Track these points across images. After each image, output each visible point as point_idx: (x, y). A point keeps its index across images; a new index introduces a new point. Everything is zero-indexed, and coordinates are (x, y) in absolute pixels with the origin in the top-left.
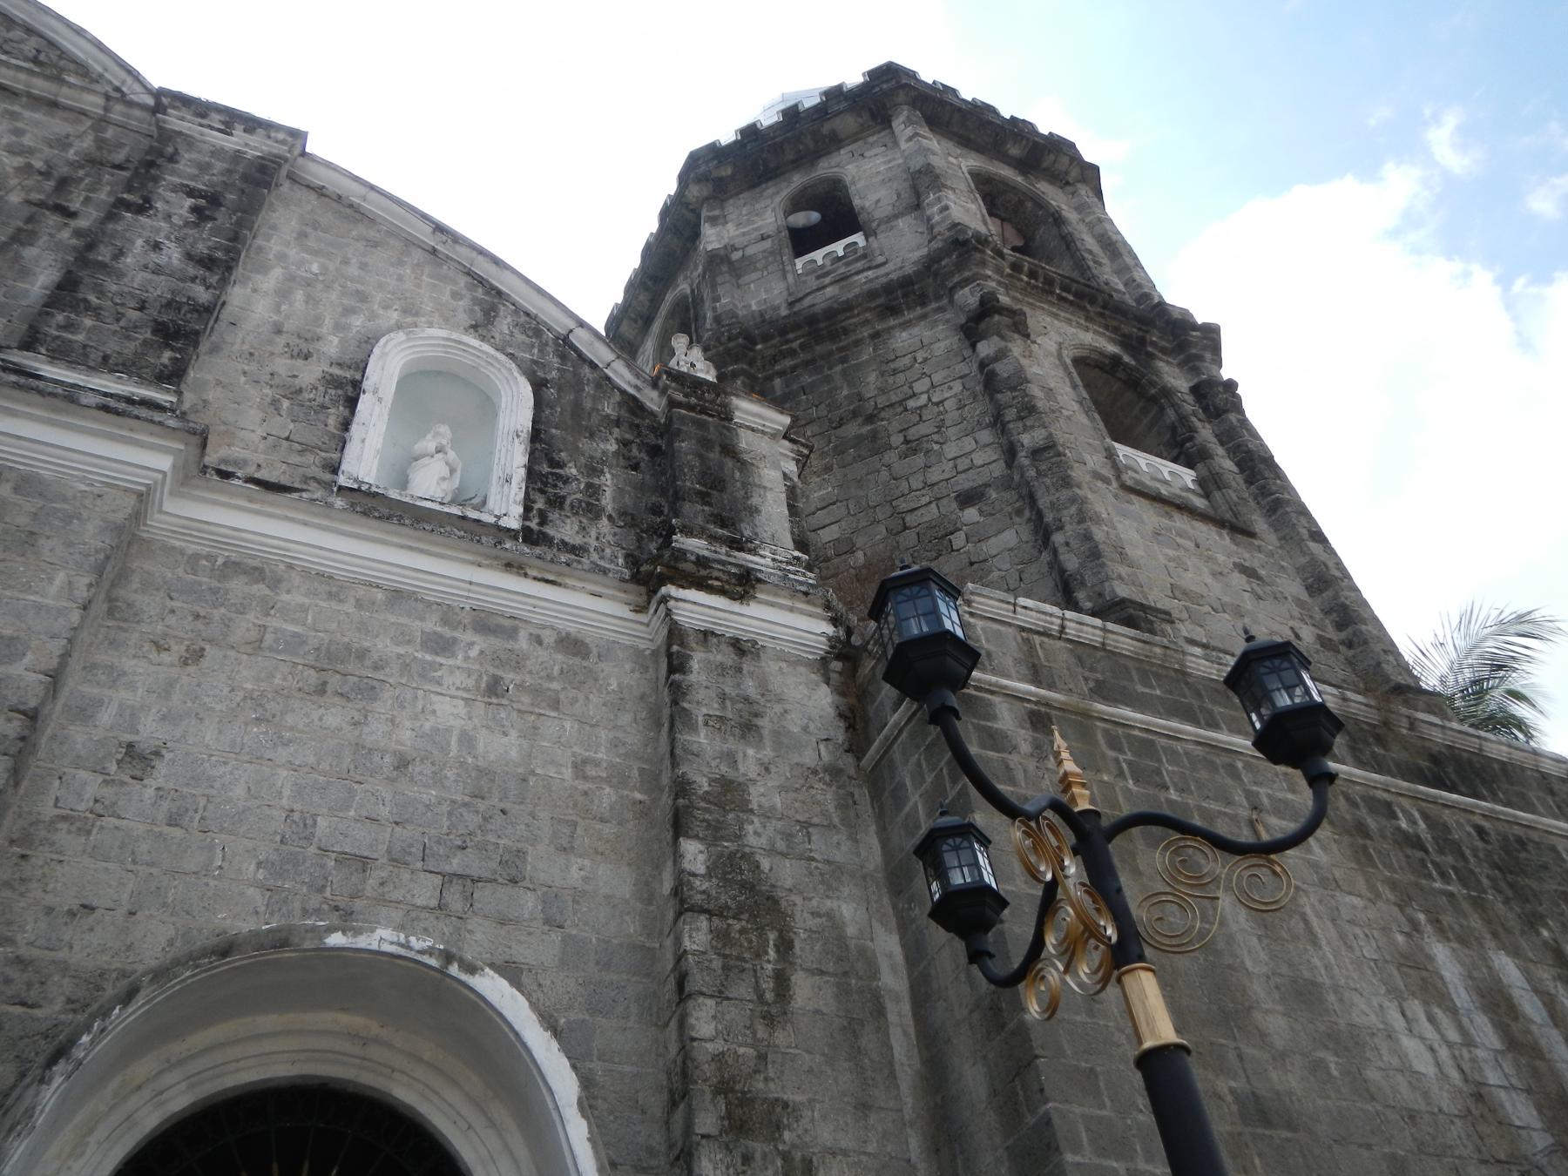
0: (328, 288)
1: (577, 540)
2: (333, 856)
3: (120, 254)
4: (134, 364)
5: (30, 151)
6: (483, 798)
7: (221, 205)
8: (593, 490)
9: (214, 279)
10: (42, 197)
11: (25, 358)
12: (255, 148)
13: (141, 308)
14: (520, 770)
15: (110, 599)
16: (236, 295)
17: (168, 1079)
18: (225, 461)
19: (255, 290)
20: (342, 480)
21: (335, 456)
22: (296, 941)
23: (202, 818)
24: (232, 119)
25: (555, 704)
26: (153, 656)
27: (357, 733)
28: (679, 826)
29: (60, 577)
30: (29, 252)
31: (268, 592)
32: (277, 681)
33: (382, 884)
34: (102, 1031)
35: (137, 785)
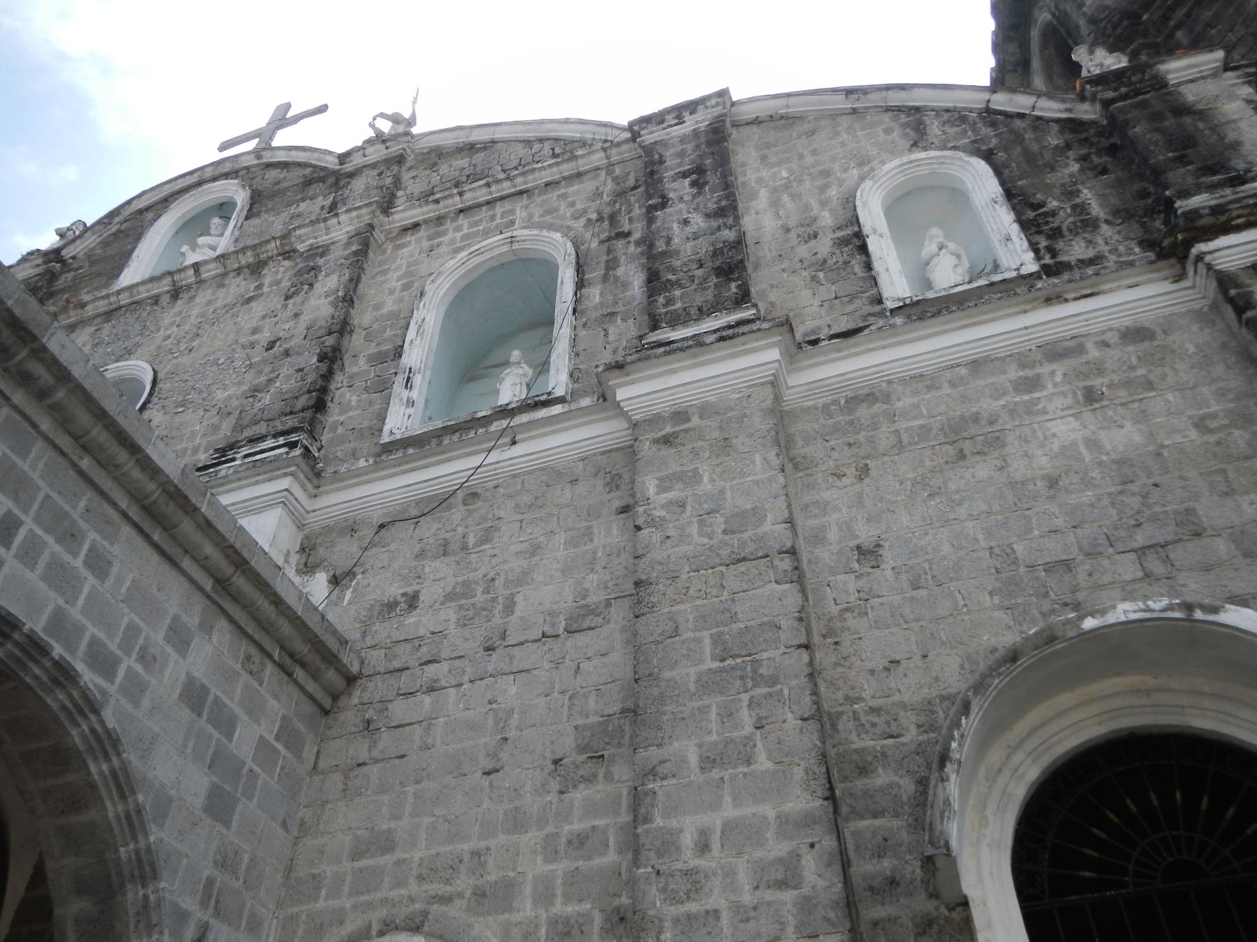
0: (801, 181)
1: (1091, 253)
2: (1041, 568)
3: (669, 240)
4: (718, 303)
5: (585, 211)
6: (1132, 482)
7: (705, 171)
8: (1080, 209)
9: (730, 221)
10: (607, 234)
11: (657, 335)
12: (704, 121)
13: (701, 266)
14: (1151, 448)
15: (791, 460)
16: (748, 222)
17: (1017, 758)
18: (806, 335)
19: (757, 213)
20: (890, 305)
21: (874, 291)
22: (1060, 634)
23: (933, 577)
24: (680, 111)
25: (1150, 386)
26: (838, 483)
27: (1005, 475)
29: (758, 458)
30: (620, 271)
31: (885, 406)
32: (928, 463)
33: (1090, 575)
34: (962, 736)
35: (877, 572)
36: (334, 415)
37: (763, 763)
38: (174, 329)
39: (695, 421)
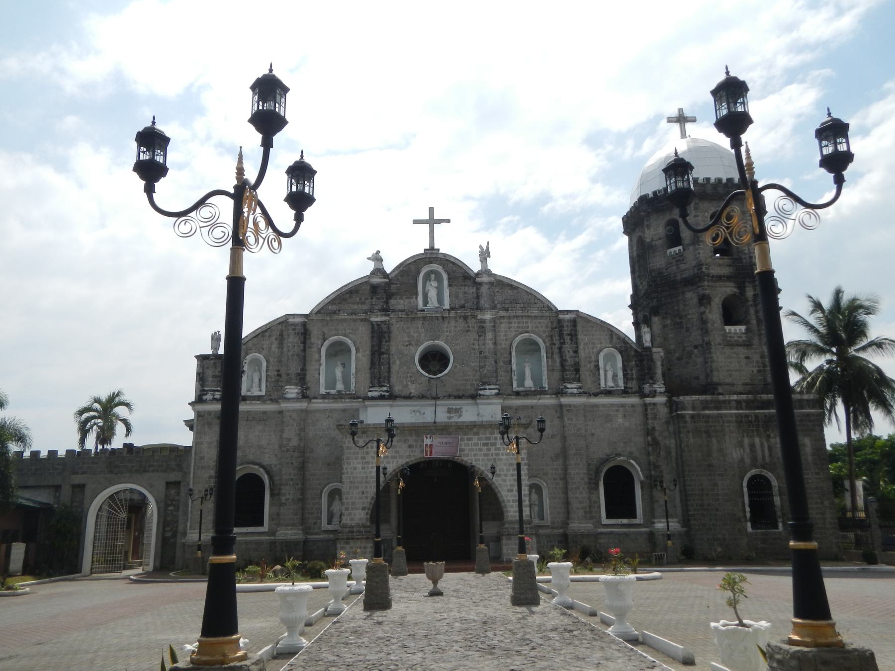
3: (566, 356)
8: (632, 374)
24: (568, 312)
28: (648, 435)
36: (499, 378)
37: (581, 466)
38: (448, 334)
39: (572, 408)
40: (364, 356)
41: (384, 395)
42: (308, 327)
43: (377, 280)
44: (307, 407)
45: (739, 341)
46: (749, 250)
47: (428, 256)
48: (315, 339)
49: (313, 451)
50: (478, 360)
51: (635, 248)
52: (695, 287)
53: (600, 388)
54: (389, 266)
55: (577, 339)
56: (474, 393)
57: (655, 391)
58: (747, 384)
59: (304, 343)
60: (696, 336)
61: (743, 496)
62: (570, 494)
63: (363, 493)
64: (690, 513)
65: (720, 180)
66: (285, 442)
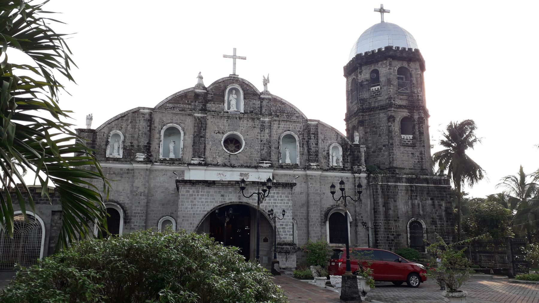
8: (348, 159)
36: (271, 157)
40: (189, 138)
41: (201, 163)
42: (152, 116)
43: (198, 91)
44: (151, 167)
45: (408, 143)
46: (417, 91)
47: (232, 78)
48: (157, 124)
49: (153, 196)
50: (259, 145)
51: (350, 85)
52: (385, 111)
53: (329, 166)
54: (207, 83)
55: (318, 137)
56: (257, 165)
57: (361, 170)
58: (412, 169)
59: (150, 126)
60: (384, 140)
61: (407, 233)
62: (310, 229)
63: (191, 223)
64: (378, 242)
65: (404, 49)
66: (135, 189)
